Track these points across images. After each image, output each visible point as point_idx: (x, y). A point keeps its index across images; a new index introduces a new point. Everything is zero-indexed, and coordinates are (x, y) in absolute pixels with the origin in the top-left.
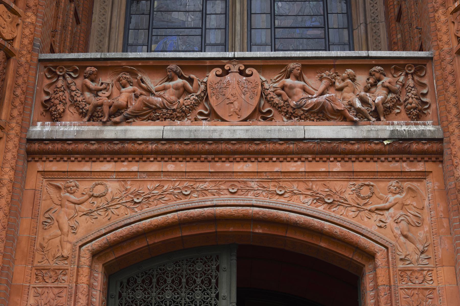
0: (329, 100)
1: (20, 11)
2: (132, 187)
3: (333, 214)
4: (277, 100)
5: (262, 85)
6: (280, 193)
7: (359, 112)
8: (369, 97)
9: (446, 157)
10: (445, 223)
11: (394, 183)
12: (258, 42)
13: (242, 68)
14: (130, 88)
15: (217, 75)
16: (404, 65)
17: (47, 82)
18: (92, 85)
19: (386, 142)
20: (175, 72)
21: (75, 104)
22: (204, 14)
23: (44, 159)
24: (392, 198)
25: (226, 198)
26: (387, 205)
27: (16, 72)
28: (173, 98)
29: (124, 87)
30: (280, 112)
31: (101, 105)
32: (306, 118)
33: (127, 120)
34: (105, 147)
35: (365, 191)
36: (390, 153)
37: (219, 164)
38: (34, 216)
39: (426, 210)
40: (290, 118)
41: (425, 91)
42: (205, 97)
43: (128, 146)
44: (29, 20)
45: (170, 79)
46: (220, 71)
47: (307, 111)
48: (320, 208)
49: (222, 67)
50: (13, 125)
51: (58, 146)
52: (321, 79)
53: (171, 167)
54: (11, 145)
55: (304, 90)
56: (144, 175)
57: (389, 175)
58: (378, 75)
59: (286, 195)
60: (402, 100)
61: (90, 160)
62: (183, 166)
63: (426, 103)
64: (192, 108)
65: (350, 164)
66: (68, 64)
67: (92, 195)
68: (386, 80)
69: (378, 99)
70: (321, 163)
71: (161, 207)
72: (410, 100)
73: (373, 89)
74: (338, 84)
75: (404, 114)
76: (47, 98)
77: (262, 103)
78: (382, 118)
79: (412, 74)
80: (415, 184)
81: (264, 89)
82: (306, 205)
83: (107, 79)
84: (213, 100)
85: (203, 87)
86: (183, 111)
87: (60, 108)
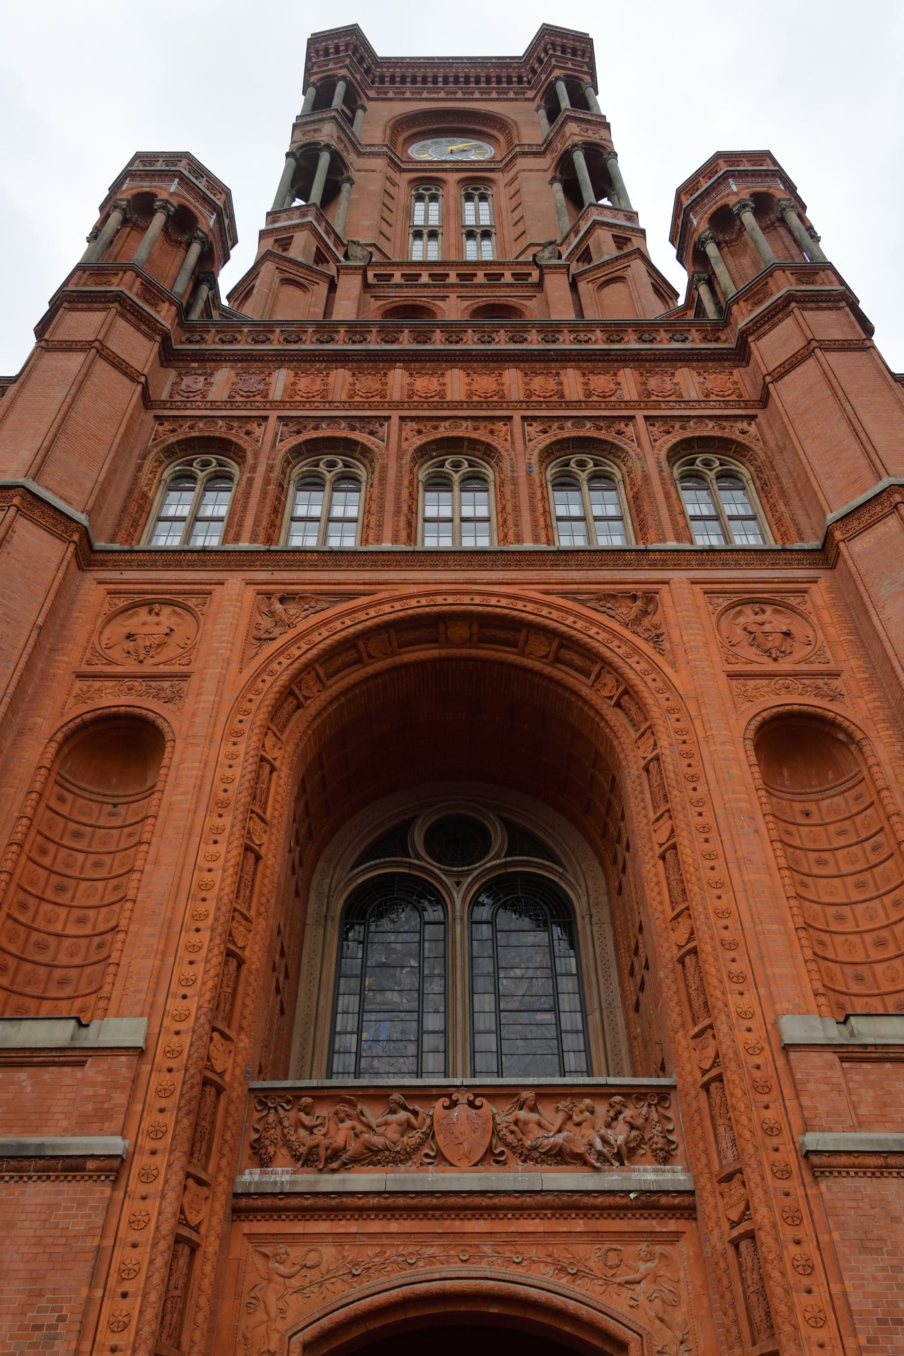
0: (567, 1140)
1: (232, 1034)
2: (350, 1253)
3: (577, 1289)
4: (510, 1138)
5: (494, 1119)
6: (518, 1260)
7: (600, 1154)
8: (610, 1134)
9: (699, 1214)
10: (705, 1300)
11: (643, 1246)
12: (482, 1028)
13: (471, 1098)
14: (348, 1123)
15: (445, 1108)
16: (646, 1095)
17: (257, 1115)
18: (307, 1120)
19: (632, 1196)
20: (398, 1104)
21: (287, 1144)
22: (421, 993)
23: (251, 1217)
24: (643, 1267)
25: (455, 1269)
26: (638, 1276)
27: (227, 1110)
28: (396, 1136)
29: (342, 1122)
30: (514, 1153)
31: (317, 1146)
32: (543, 1161)
33: (344, 1167)
34: (322, 1202)
35: (613, 1259)
36: (638, 1208)
37: (448, 1223)
38: (238, 1296)
39: (682, 1284)
40: (524, 1161)
41: (670, 1127)
42: (430, 1135)
43: (347, 1201)
44: (241, 1045)
45: (393, 1112)
46: (447, 1102)
47: (544, 1153)
48: (563, 1281)
49: (449, 1096)
50: (221, 1179)
51: (268, 1202)
52: (557, 1110)
53: (394, 1227)
54: (217, 1206)
55: (539, 1125)
56: (364, 1238)
57: (637, 1235)
58: (618, 1107)
59: (524, 1264)
60: (647, 1137)
61: (304, 1219)
62: (407, 1226)
63: (673, 1142)
64: (417, 1148)
65: (593, 1221)
66: (281, 1093)
67: (305, 1266)
68: (627, 1113)
69: (621, 1139)
70: (561, 1221)
71: (382, 1281)
72: (655, 1139)
73: (614, 1124)
74: (577, 1118)
75: (649, 1155)
76: (256, 1136)
77: (494, 1142)
78: (626, 1162)
79: (655, 1105)
80: (667, 1249)
81: (495, 1125)
82: (547, 1277)
83: (324, 1111)
84: (440, 1138)
85: (428, 1121)
86: (407, 1153)
87: (271, 1149)
